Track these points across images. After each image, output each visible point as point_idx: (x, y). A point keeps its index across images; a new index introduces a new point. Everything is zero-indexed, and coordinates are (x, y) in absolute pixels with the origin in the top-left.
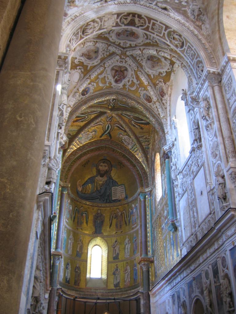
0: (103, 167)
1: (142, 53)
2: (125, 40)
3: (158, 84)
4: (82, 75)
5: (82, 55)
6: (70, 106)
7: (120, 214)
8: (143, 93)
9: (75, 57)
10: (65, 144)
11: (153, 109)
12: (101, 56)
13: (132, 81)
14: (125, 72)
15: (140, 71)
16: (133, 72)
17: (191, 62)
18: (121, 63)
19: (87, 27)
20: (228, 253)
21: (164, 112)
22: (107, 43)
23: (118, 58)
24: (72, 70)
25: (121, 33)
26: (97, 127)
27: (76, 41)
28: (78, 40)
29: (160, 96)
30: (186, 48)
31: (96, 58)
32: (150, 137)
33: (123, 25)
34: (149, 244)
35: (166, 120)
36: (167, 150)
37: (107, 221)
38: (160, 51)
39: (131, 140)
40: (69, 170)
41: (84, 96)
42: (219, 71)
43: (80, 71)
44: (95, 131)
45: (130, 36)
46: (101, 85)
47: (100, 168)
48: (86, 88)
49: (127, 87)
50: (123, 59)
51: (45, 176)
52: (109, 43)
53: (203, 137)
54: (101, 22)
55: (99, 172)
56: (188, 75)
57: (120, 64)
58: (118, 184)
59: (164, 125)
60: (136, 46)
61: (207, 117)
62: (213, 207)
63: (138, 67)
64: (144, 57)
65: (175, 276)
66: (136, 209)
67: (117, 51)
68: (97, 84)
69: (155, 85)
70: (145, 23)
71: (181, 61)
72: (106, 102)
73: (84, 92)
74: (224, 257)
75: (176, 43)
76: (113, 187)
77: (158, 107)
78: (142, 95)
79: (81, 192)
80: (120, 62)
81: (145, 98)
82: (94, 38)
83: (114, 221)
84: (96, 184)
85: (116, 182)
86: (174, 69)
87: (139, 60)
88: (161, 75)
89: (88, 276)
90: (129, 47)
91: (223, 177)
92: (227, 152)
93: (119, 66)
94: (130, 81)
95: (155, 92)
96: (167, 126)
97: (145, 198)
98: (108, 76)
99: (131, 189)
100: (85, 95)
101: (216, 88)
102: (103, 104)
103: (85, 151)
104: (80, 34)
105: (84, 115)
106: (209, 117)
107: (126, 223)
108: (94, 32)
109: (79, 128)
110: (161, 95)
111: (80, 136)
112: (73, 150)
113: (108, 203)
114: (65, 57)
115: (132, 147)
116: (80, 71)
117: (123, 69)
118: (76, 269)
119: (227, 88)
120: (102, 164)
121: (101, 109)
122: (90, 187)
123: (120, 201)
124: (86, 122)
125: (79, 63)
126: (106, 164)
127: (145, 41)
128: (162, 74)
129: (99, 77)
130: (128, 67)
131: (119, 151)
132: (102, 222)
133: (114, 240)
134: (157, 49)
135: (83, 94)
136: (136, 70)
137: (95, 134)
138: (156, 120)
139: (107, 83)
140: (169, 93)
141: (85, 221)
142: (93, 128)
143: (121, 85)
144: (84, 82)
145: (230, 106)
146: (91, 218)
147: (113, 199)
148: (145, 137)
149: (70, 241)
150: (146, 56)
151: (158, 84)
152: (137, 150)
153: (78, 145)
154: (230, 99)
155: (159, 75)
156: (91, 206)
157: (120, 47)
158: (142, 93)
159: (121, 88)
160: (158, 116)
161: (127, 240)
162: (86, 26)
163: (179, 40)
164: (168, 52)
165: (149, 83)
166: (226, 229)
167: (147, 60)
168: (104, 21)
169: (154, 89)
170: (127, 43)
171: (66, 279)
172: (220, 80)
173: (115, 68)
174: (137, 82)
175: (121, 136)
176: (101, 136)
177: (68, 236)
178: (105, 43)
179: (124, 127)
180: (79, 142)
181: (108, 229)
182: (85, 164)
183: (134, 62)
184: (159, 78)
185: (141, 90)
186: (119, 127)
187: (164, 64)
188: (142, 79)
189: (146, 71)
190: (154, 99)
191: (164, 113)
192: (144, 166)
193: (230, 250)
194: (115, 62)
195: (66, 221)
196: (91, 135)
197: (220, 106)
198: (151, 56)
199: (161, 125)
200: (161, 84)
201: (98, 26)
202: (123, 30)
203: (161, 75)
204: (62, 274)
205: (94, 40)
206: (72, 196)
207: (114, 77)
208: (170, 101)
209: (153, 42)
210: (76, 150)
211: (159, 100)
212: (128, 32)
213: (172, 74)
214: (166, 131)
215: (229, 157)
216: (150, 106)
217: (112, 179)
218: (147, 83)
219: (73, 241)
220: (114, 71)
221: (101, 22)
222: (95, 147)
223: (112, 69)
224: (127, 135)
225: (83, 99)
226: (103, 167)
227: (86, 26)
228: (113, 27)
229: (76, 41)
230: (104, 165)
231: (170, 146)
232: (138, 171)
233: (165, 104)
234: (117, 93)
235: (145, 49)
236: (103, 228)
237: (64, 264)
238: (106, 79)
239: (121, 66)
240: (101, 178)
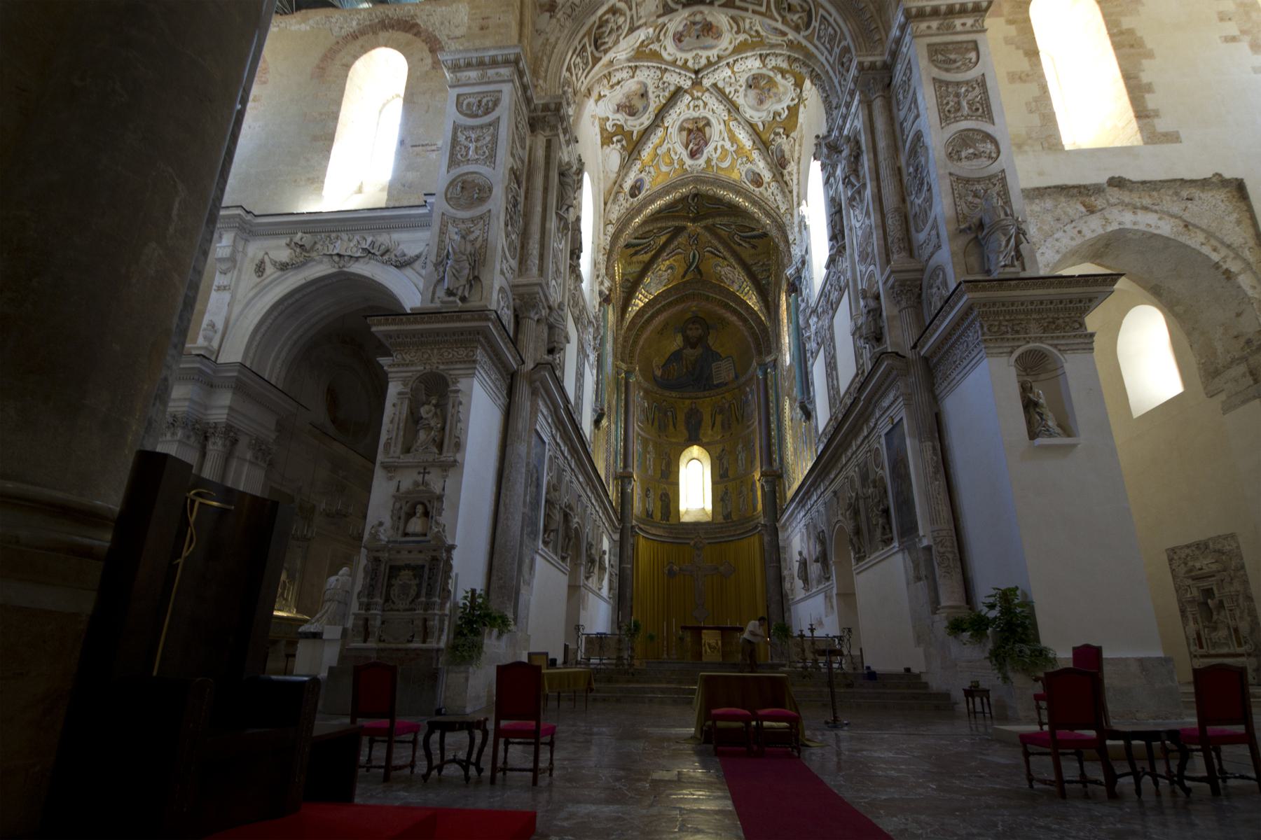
0: (694, 332)
1: (733, 72)
2: (695, 49)
3: (773, 140)
4: (625, 154)
5: (616, 108)
6: (611, 223)
7: (727, 405)
8: (745, 170)
9: (603, 116)
10: (610, 294)
11: (767, 199)
12: (655, 102)
13: (722, 146)
14: (707, 129)
15: (736, 119)
16: (722, 127)
17: (829, 57)
18: (697, 109)
19: (601, 30)
20: (883, 440)
21: (788, 201)
22: (659, 65)
23: (687, 98)
24: (605, 147)
25: (685, 33)
26: (674, 260)
27: (584, 70)
28: (589, 67)
30: (817, 25)
31: (646, 108)
32: (770, 262)
33: (680, 7)
34: (775, 448)
35: (792, 215)
37: (707, 419)
38: (768, 55)
39: (737, 274)
40: (635, 342)
41: (636, 199)
42: (886, 57)
43: (619, 146)
45: (704, 35)
46: (664, 169)
47: (689, 332)
48: (636, 182)
49: (713, 163)
50: (698, 98)
52: (663, 66)
53: (848, 225)
54: (631, 9)
55: (686, 339)
56: (825, 95)
57: (694, 113)
58: (721, 356)
59: (788, 228)
60: (720, 58)
61: (853, 179)
62: (861, 362)
63: (729, 112)
64: (739, 84)
65: (808, 494)
66: (753, 396)
67: (682, 83)
68: (658, 167)
71: (809, 66)
72: (681, 206)
73: (636, 190)
74: (877, 448)
75: (795, 17)
76: (714, 364)
77: (775, 192)
78: (743, 174)
79: (661, 377)
80: (694, 110)
81: (750, 179)
82: (629, 60)
83: (719, 418)
84: (684, 362)
85: (717, 353)
86: (804, 95)
87: (730, 92)
88: (778, 118)
90: (706, 67)
91: (877, 297)
92: (889, 242)
93: (694, 119)
94: (719, 147)
95: (769, 160)
96: (792, 228)
97: (765, 373)
98: (675, 145)
100: (636, 196)
101: (878, 104)
102: (677, 211)
103: (658, 307)
104: (589, 50)
105: (647, 240)
106: (858, 176)
107: (737, 420)
108: (621, 38)
109: (642, 265)
110: (780, 165)
111: (647, 280)
112: (638, 308)
113: (708, 390)
114: (556, 104)
115: (740, 287)
116: (619, 146)
117: (701, 124)
119: (901, 96)
120: (690, 326)
121: (674, 221)
122: (676, 367)
123: (726, 384)
124: (653, 252)
125: (615, 128)
126: (697, 326)
127: (736, 39)
128: (780, 115)
129: (659, 152)
130: (709, 115)
131: (718, 297)
133: (719, 448)
134: (762, 52)
136: (726, 118)
137: (673, 274)
138: (772, 222)
139: (676, 162)
140: (796, 155)
141: (671, 423)
142: (667, 262)
143: (702, 161)
144: (630, 167)
145: (905, 137)
146: (681, 417)
147: (715, 383)
148: (761, 263)
149: (648, 456)
150: (742, 81)
151: (773, 140)
152: (748, 291)
153: (646, 297)
154: (905, 119)
155: (774, 118)
156: (679, 398)
157: (687, 69)
158: (744, 169)
159: (703, 169)
160: (777, 210)
161: (740, 446)
162: (600, 27)
163: (801, 7)
164: (784, 52)
165: (754, 142)
166: (882, 396)
167: (746, 90)
168: (636, 5)
169: (766, 154)
170: (701, 57)
172: (886, 81)
173: (686, 125)
174: (732, 146)
175: (719, 268)
176: (684, 276)
178: (654, 67)
179: (722, 251)
180: (647, 292)
181: (710, 432)
182: (662, 329)
183: (721, 102)
184: (774, 125)
185: (740, 164)
186: (712, 252)
187: (781, 89)
188: (741, 137)
189: (747, 116)
191: (786, 203)
192: (763, 318)
193: (887, 434)
194: (682, 112)
197: (882, 144)
198: (753, 75)
199: (782, 228)
201: (625, 21)
202: (685, 22)
203: (778, 118)
205: (630, 64)
206: (646, 385)
207: (687, 148)
208: (799, 173)
209: (751, 36)
210: (643, 307)
211: (777, 175)
212: (698, 27)
213: (802, 109)
214: (791, 238)
215: (893, 253)
216: (760, 193)
218: (750, 143)
220: (685, 133)
221: (631, 9)
222: (675, 297)
223: (681, 129)
224: (728, 265)
225: (635, 204)
227: (600, 27)
228: (659, 16)
229: (584, 70)
231: (797, 268)
232: (753, 328)
234: (697, 180)
235: (737, 60)
239: (699, 118)
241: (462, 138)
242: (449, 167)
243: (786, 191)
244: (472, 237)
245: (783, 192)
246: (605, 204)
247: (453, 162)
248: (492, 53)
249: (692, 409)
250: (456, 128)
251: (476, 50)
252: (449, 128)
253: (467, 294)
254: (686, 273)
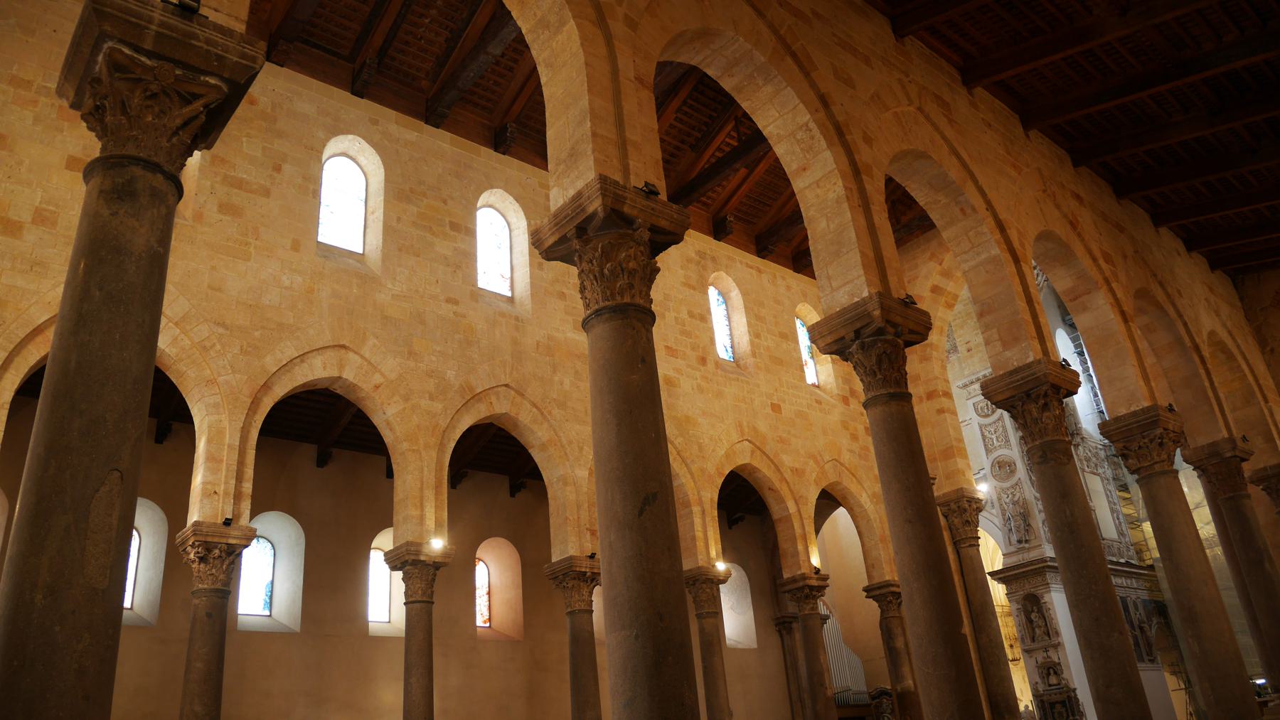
241: (986, 434)
242: (987, 454)
244: (1016, 499)
247: (988, 451)
248: (983, 373)
250: (981, 427)
251: (973, 374)
252: (977, 428)
253: (1027, 538)
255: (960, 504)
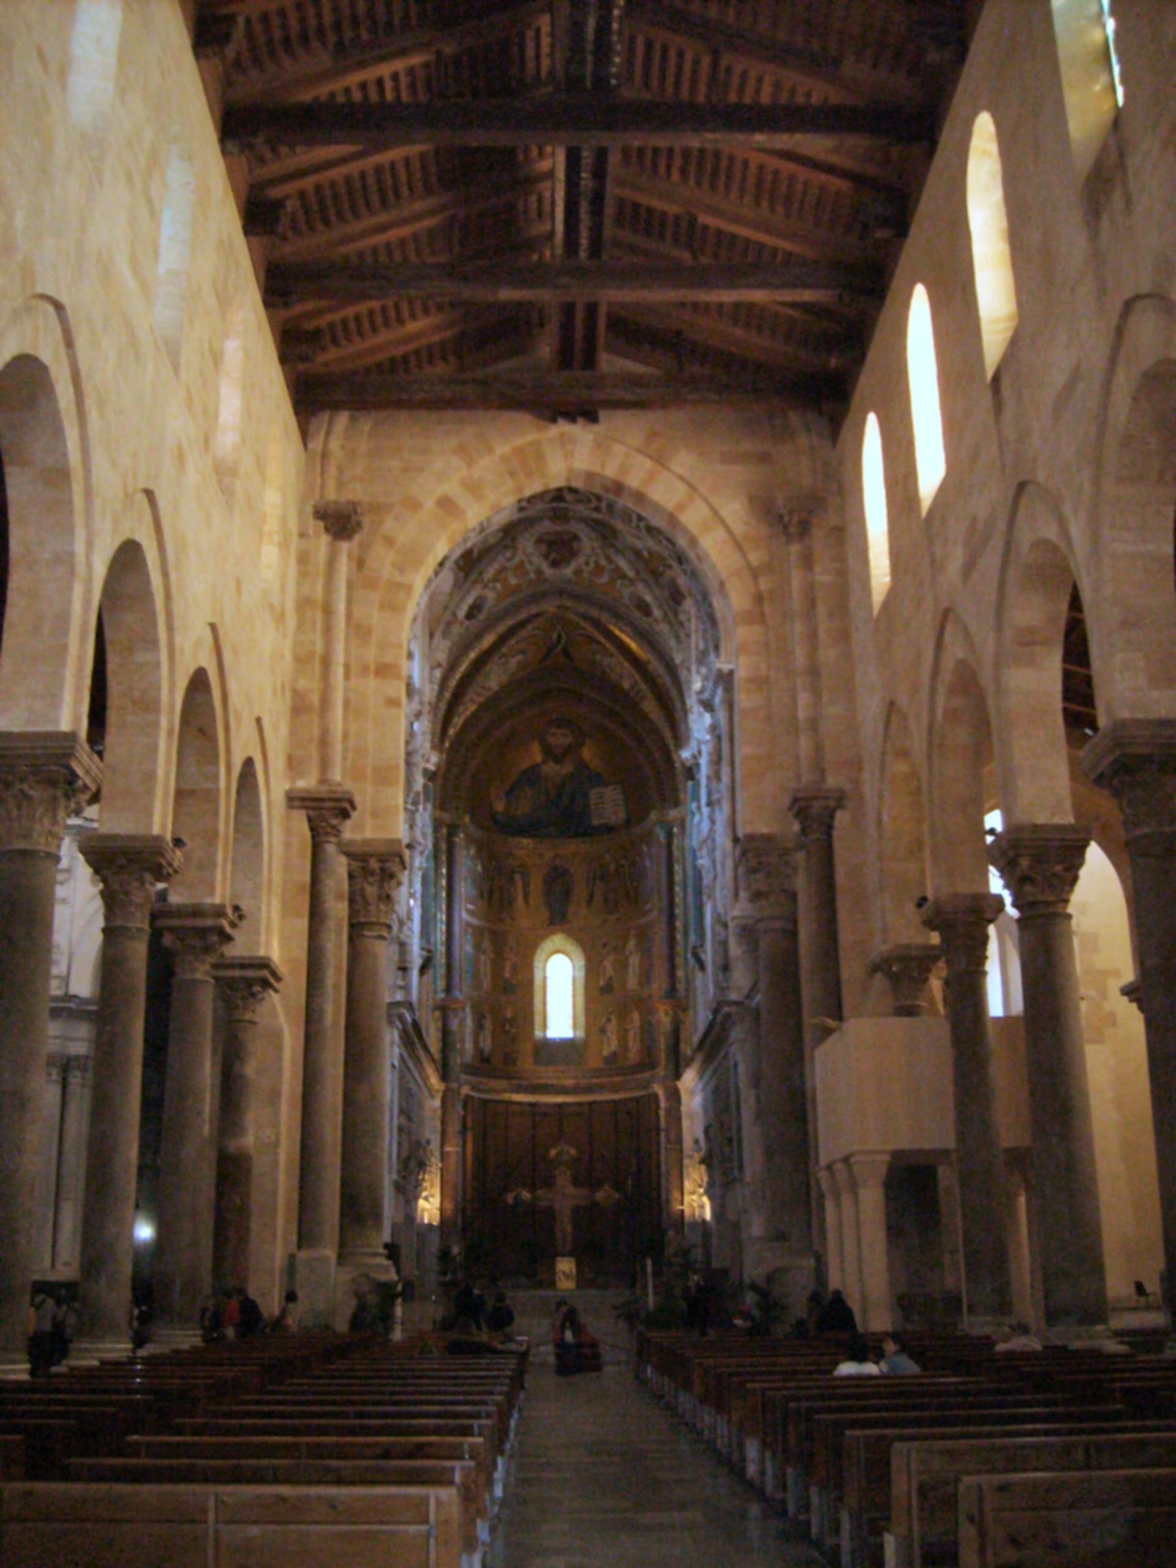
3: (664, 571)
6: (439, 665)
7: (612, 867)
15: (613, 546)
29: (671, 603)
35: (689, 670)
36: (687, 759)
37: (580, 891)
41: (474, 621)
44: (523, 652)
47: (552, 740)
51: (410, 690)
55: (548, 752)
63: (604, 538)
69: (656, 575)
70: (589, 500)
85: (598, 775)
89: (538, 1033)
97: (670, 835)
99: (638, 808)
118: (504, 1026)
120: (553, 730)
123: (610, 829)
132: (567, 893)
135: (470, 616)
144: (468, 592)
149: (483, 958)
171: (482, 1052)
177: (478, 947)
180: (483, 687)
190: (657, 613)
195: (468, 911)
196: (513, 663)
200: (669, 573)
204: (469, 1046)
207: (546, 557)
217: (588, 768)
219: (492, 956)
226: (560, 738)
230: (559, 731)
233: (686, 624)
236: (572, 909)
237: (473, 1020)
238: (528, 566)
240: (556, 767)
243: (682, 634)
245: (677, 637)
246: (432, 635)
249: (555, 868)
254: (547, 655)
255: (388, 865)
